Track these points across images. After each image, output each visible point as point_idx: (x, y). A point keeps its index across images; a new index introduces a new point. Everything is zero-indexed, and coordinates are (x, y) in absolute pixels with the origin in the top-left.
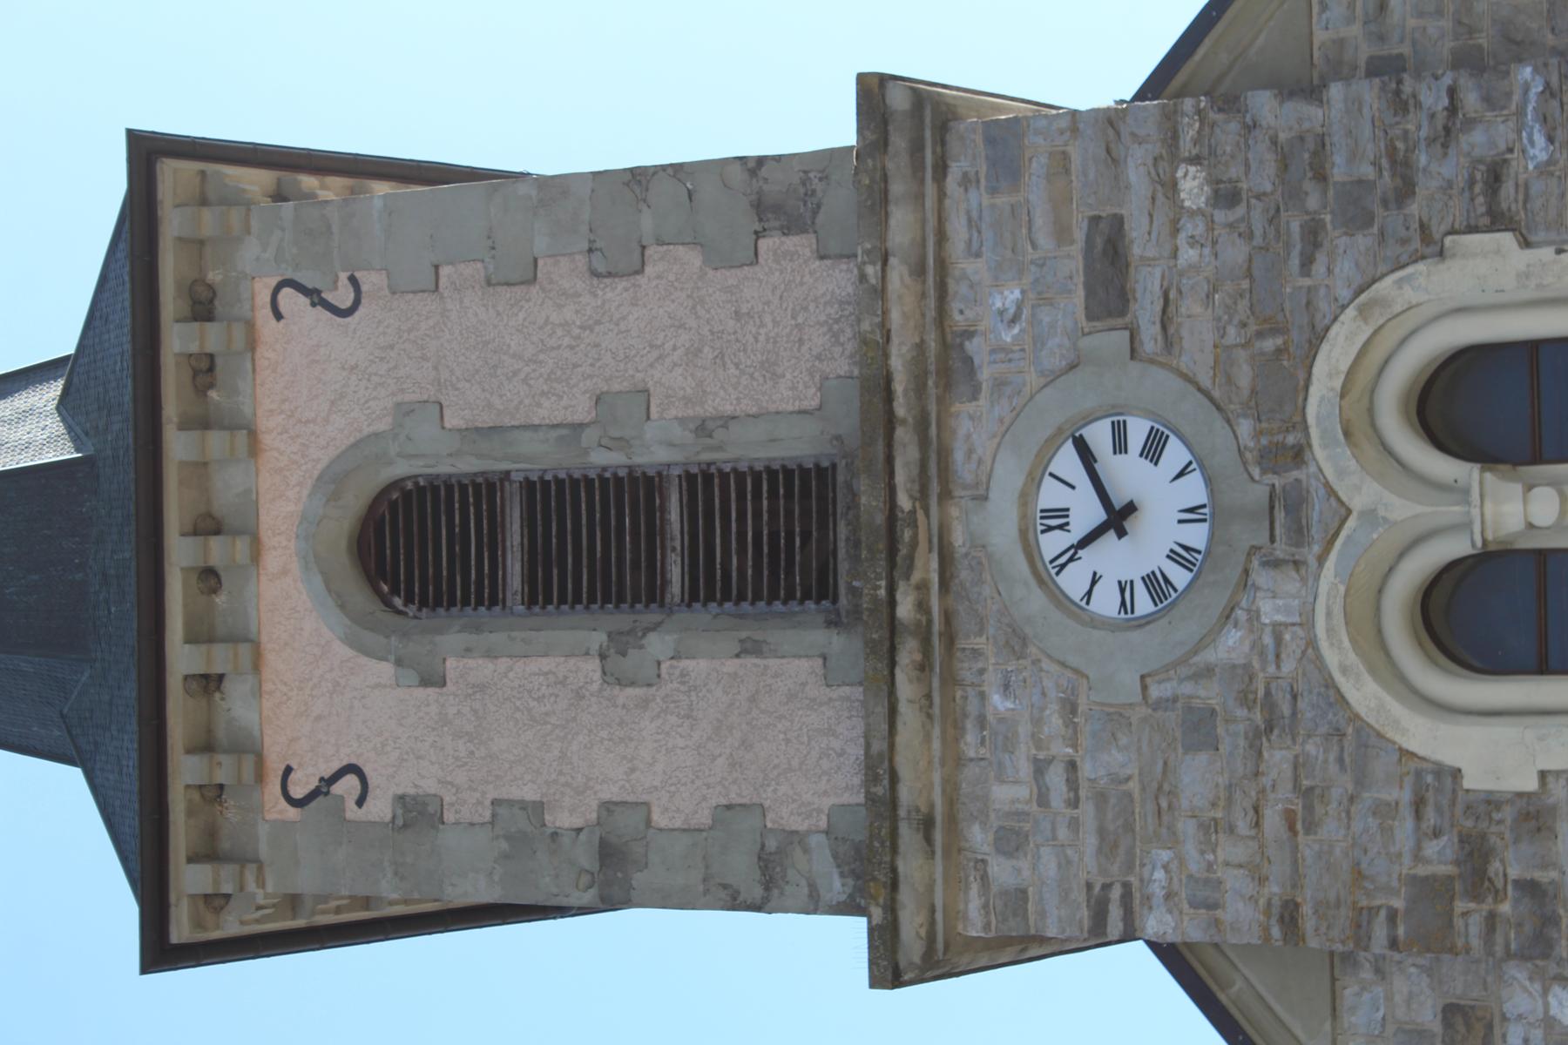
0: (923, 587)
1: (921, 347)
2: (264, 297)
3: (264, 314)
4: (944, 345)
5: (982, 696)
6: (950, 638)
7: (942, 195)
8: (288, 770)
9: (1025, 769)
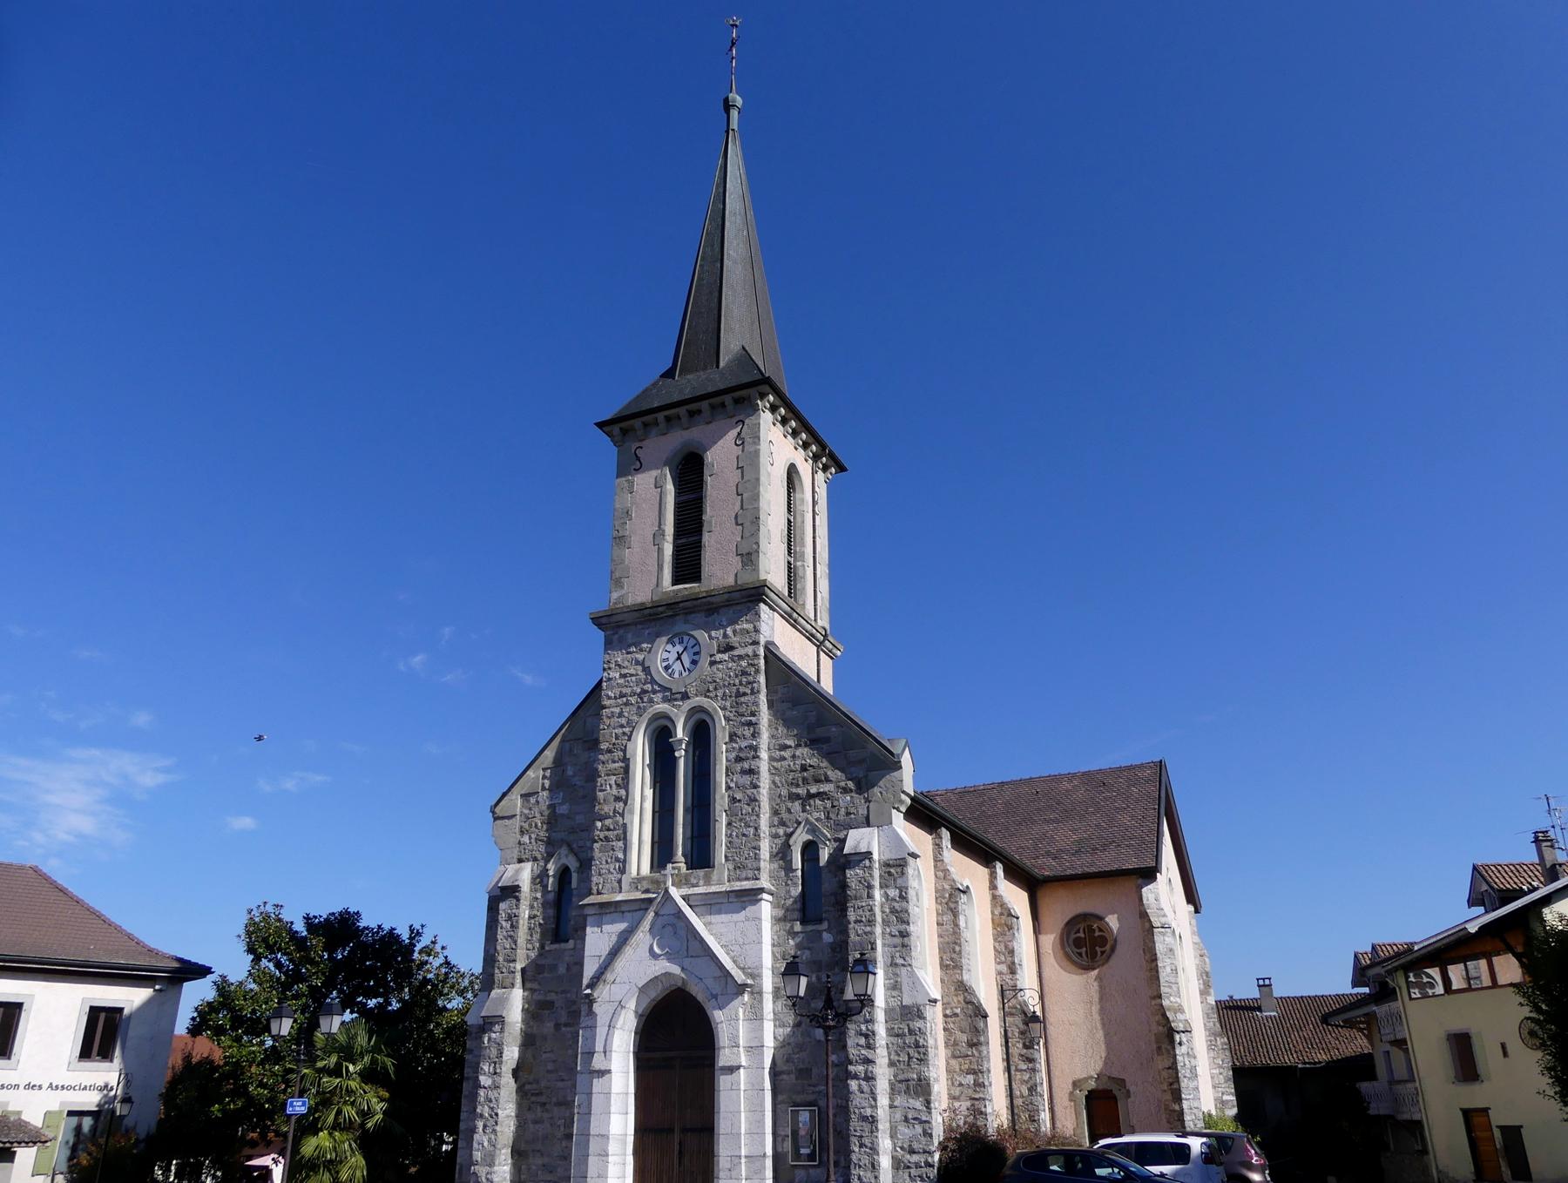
0: (665, 612)
1: (713, 603)
2: (741, 418)
3: (737, 418)
4: (716, 608)
5: (648, 628)
6: (658, 619)
7: (745, 602)
8: (641, 448)
9: (634, 641)
